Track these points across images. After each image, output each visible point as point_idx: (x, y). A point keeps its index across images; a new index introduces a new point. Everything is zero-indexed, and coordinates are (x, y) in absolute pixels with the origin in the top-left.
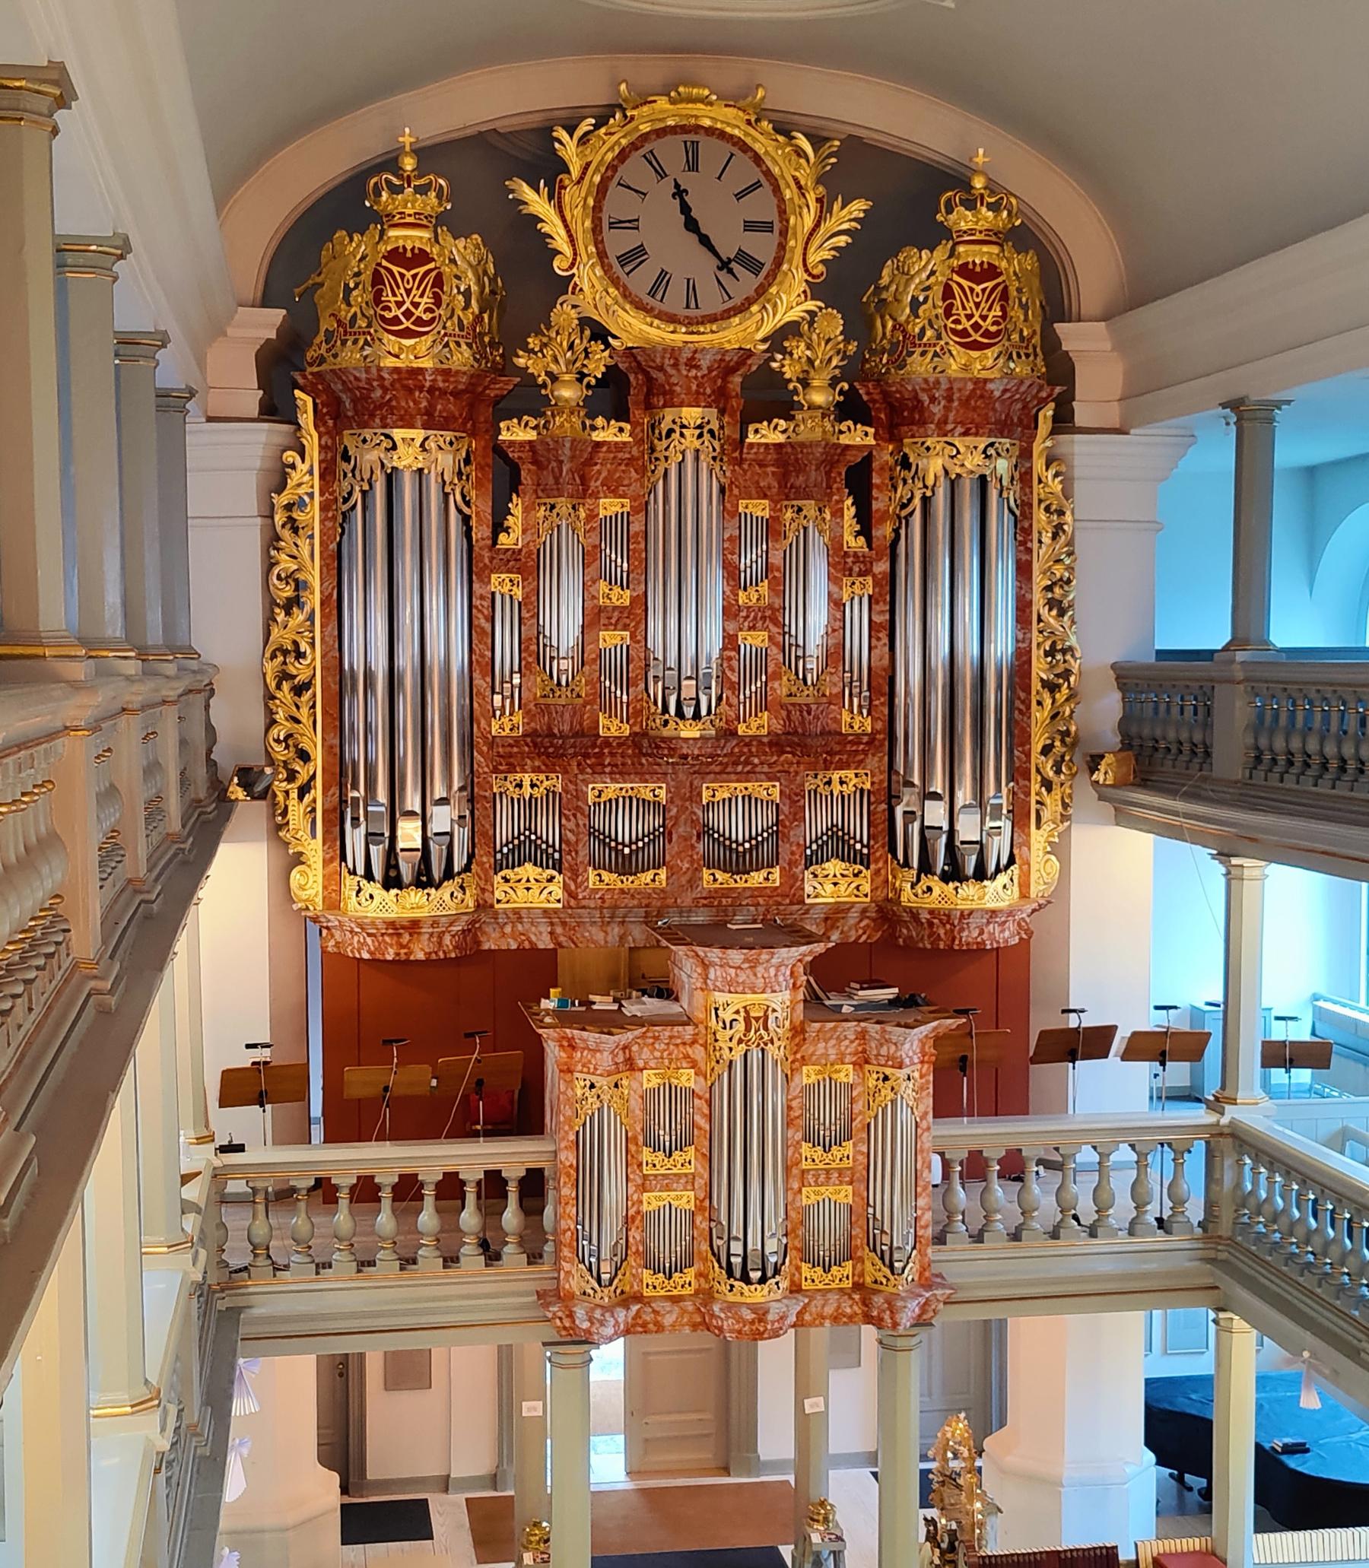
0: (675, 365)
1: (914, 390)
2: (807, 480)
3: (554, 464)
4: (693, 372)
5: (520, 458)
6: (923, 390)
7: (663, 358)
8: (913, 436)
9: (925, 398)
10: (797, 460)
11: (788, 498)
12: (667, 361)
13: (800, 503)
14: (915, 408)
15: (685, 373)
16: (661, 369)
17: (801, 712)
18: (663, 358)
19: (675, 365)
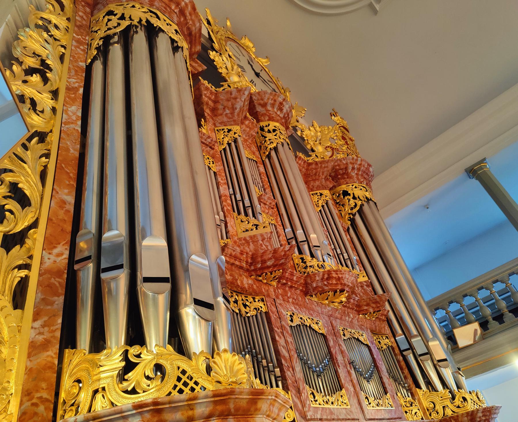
0: (273, 105)
1: (347, 164)
2: (321, 183)
3: (228, 111)
4: (279, 113)
5: (207, 104)
6: (351, 163)
7: (268, 99)
8: (347, 183)
9: (350, 167)
10: (315, 174)
11: (312, 190)
12: (270, 101)
13: (321, 191)
14: (344, 174)
15: (275, 110)
16: (264, 105)
17: (362, 287)
18: (268, 99)
19: (273, 105)
